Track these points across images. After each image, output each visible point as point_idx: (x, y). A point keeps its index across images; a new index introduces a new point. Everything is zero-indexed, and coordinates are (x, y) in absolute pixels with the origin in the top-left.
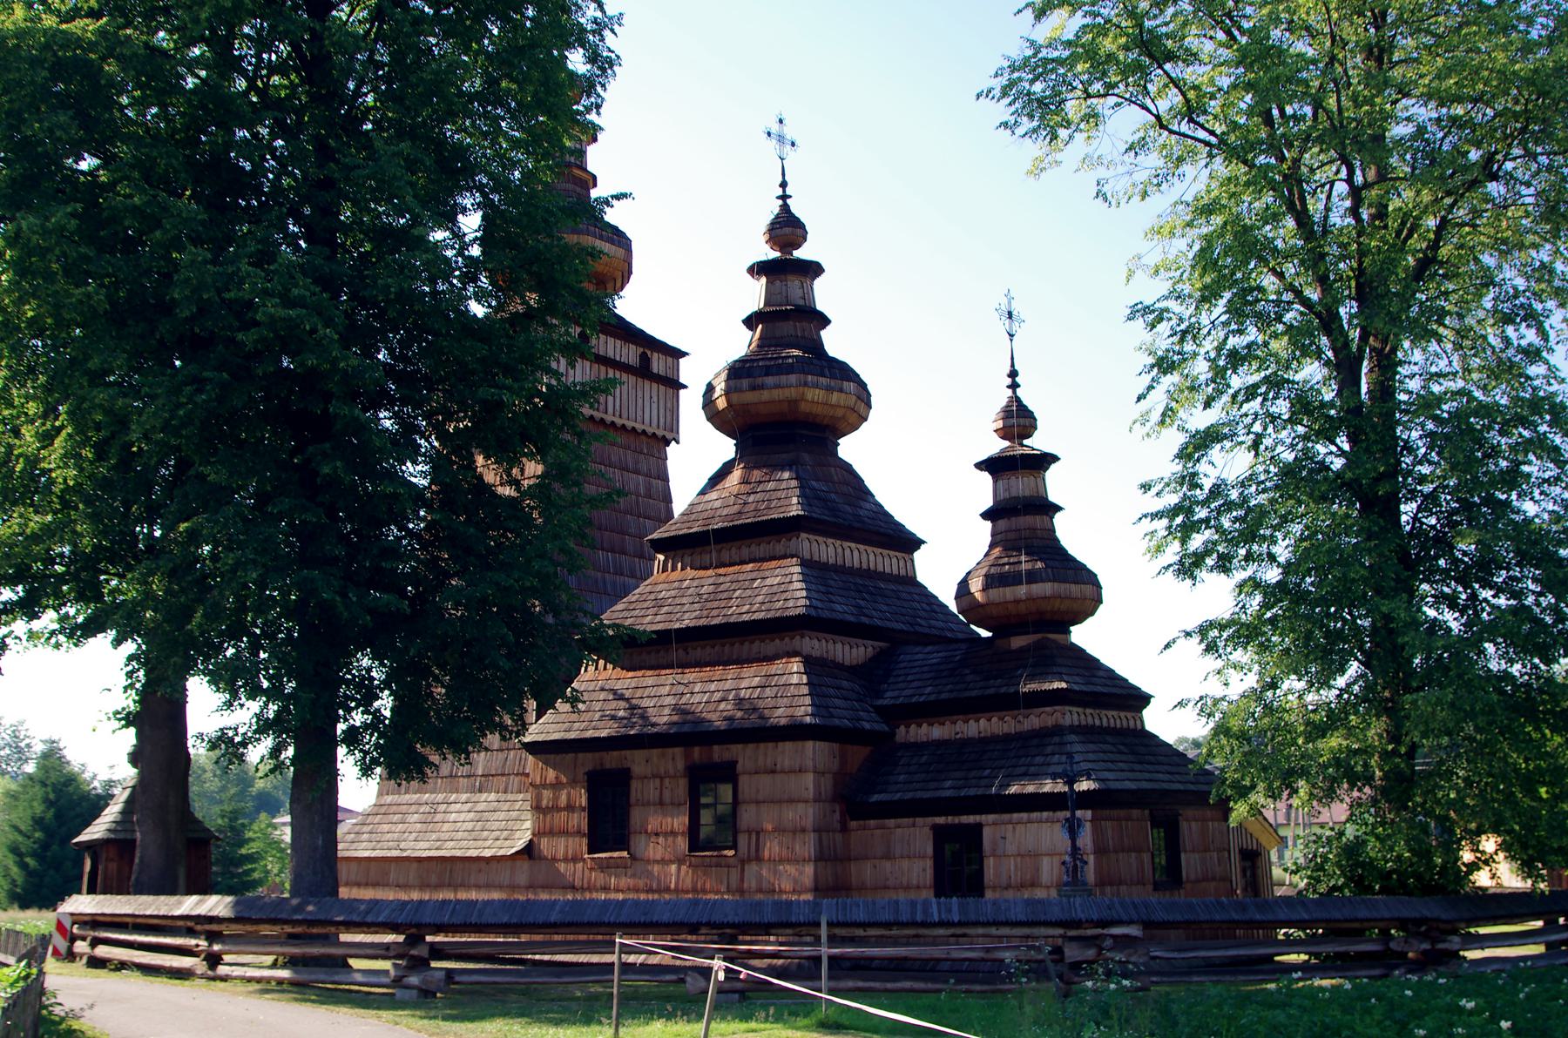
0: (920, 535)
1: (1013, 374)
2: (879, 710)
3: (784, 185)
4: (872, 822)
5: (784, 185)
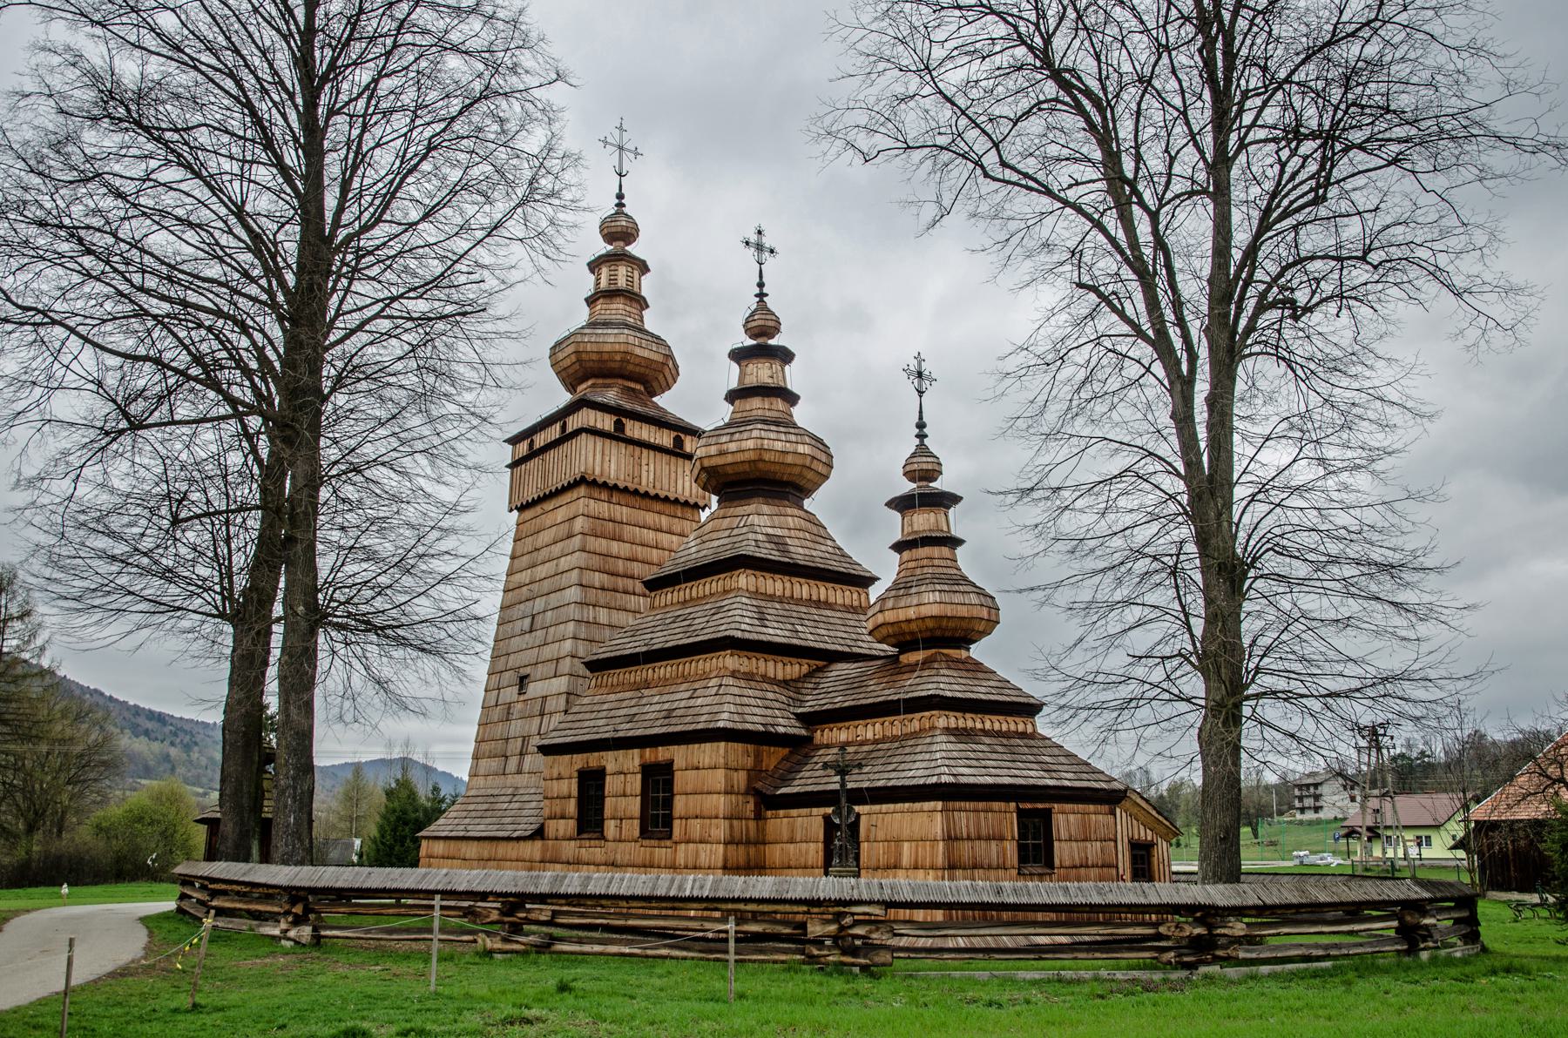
0: (875, 573)
1: (921, 425)
2: (799, 717)
3: (761, 285)
4: (782, 812)
5: (761, 285)
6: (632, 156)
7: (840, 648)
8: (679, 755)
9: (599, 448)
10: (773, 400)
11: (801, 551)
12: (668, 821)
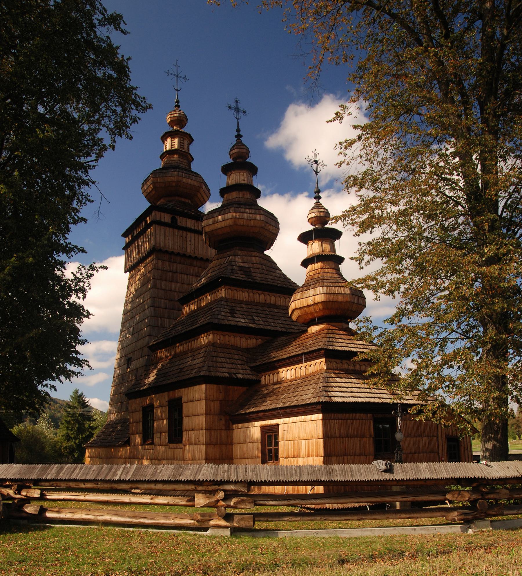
3: (238, 130)
4: (240, 425)
5: (238, 130)
6: (183, 80)
7: (280, 329)
9: (162, 232)
10: (245, 192)
11: (260, 275)
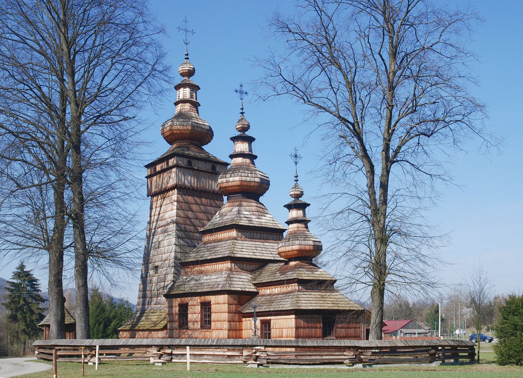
8: (213, 299)
12: (210, 322)
